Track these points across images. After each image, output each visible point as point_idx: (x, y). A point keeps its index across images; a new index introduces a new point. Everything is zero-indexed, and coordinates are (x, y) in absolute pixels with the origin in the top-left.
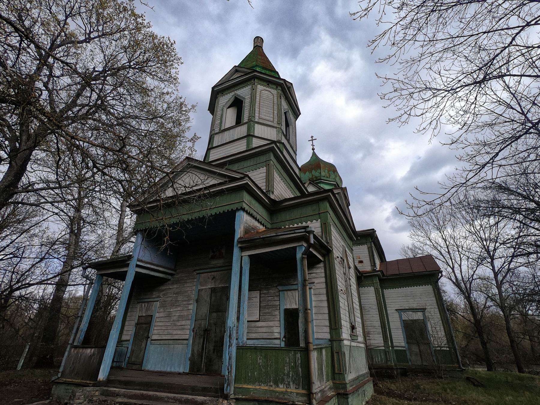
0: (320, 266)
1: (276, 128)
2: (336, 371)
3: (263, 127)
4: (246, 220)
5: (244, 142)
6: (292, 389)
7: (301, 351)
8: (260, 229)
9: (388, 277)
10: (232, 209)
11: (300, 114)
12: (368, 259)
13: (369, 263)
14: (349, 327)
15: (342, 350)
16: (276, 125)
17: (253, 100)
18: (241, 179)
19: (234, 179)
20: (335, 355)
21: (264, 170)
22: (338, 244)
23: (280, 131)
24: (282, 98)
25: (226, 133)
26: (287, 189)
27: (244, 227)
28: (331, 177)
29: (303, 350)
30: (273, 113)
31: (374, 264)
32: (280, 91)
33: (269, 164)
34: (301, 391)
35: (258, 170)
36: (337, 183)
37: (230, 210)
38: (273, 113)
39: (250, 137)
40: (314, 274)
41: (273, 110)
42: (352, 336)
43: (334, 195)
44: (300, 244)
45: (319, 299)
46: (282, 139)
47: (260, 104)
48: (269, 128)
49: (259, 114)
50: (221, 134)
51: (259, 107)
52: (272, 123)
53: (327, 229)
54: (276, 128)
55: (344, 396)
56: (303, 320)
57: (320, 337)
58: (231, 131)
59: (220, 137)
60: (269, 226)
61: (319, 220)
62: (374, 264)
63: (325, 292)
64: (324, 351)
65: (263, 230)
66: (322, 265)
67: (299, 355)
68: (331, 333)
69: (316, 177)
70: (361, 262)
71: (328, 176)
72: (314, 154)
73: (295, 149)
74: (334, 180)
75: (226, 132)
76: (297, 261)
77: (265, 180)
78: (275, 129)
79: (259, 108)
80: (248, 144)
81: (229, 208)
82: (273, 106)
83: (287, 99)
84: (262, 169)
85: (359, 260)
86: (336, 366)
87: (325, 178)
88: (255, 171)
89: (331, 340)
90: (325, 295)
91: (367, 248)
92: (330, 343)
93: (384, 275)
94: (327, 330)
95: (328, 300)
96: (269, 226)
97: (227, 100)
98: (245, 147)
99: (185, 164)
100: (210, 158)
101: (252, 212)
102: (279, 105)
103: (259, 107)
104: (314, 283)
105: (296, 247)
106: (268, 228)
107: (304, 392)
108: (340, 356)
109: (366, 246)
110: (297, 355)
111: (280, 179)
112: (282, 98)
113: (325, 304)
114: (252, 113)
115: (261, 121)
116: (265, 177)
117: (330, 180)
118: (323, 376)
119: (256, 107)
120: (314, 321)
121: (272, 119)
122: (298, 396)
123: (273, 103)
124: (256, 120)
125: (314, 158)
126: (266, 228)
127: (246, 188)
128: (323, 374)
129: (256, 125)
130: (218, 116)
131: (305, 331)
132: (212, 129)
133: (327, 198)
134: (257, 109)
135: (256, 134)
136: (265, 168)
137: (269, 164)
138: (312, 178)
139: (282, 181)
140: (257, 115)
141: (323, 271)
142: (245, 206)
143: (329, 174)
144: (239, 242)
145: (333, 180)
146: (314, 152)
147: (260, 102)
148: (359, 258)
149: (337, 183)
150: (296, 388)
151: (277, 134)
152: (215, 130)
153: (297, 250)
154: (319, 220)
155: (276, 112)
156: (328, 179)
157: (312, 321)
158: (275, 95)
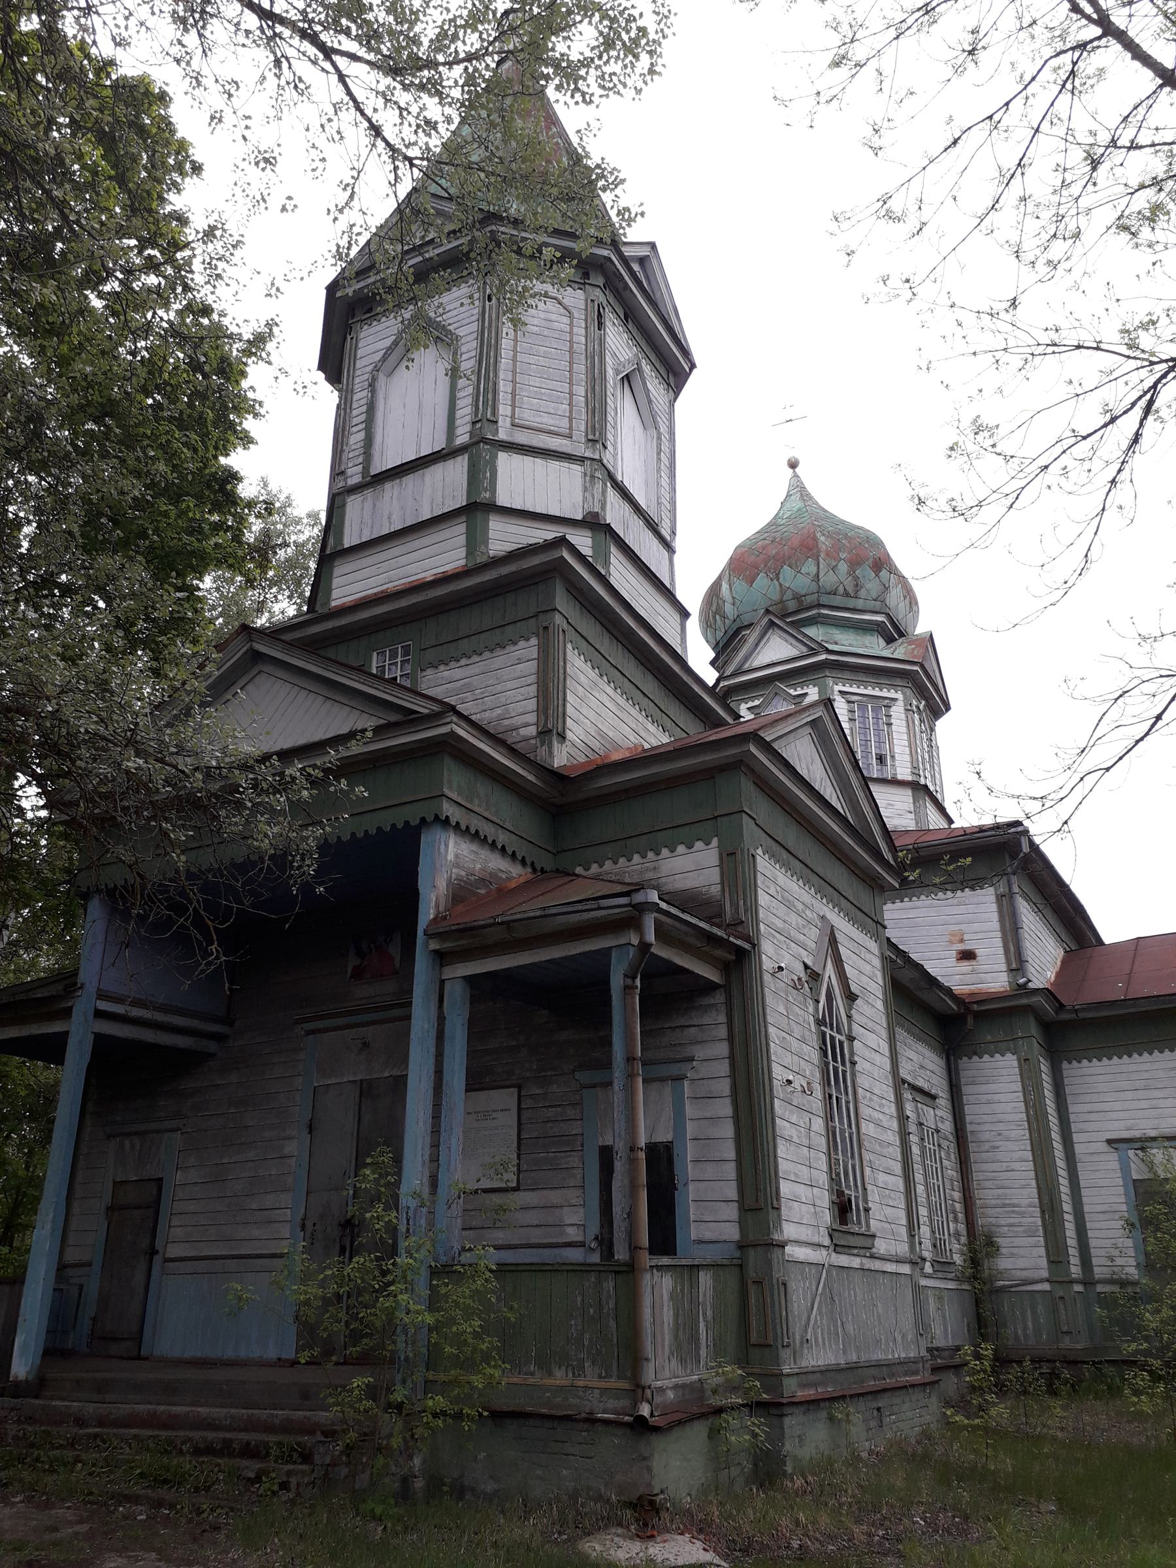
0: (712, 1001)
1: (581, 460)
2: (754, 1338)
3: (528, 460)
4: (457, 856)
5: (456, 535)
6: (591, 1378)
7: (616, 1273)
8: (509, 879)
9: (1081, 1015)
10: (407, 823)
11: (693, 366)
12: (998, 942)
13: (1001, 958)
14: (826, 1203)
15: (776, 1275)
16: (581, 450)
17: (489, 346)
18: (434, 717)
19: (411, 719)
20: (752, 1290)
21: (528, 649)
22: (793, 919)
23: (598, 474)
24: (610, 318)
25: (390, 489)
26: (628, 706)
27: (449, 882)
28: (862, 594)
29: (622, 1269)
30: (571, 394)
31: (1017, 962)
32: (598, 292)
33: (546, 628)
34: (614, 1383)
35: (510, 648)
36: (888, 616)
37: (400, 826)
38: (571, 394)
39: (479, 516)
40: (693, 1030)
41: (571, 384)
42: (836, 1234)
43: (767, 747)
44: (622, 941)
45: (708, 1115)
46: (603, 507)
47: (514, 360)
48: (554, 465)
49: (513, 406)
50: (369, 493)
51: (514, 372)
52: (565, 442)
53: (740, 874)
54: (581, 460)
55: (774, 1411)
56: (626, 1182)
57: (708, 1236)
58: (409, 480)
59: (368, 504)
60: (545, 861)
61: (715, 842)
62: (1017, 962)
63: (727, 1091)
64: (705, 1280)
65: (522, 880)
66: (719, 998)
67: (612, 1284)
68: (742, 1224)
69: (798, 597)
70: (967, 955)
71: (850, 590)
72: (798, 489)
73: (665, 533)
74: (877, 605)
75: (388, 486)
76: (610, 997)
77: (533, 690)
78: (577, 469)
79: (514, 381)
80: (475, 540)
81: (397, 818)
82: (571, 363)
83: (631, 317)
84: (522, 644)
85: (961, 947)
86: (754, 1322)
87: (837, 600)
88: (499, 652)
89: (742, 1246)
90: (728, 1101)
91: (993, 898)
92: (737, 1254)
93: (1062, 1006)
94: (732, 1212)
95: (736, 1118)
96: (545, 861)
97: (388, 342)
98: (462, 552)
99: (239, 650)
100: (335, 594)
101: (476, 824)
102: (596, 355)
103: (514, 372)
104: (692, 1059)
105: (611, 948)
106: (543, 871)
107: (624, 1385)
108: (767, 1294)
109: (991, 890)
110: (605, 1284)
111: (593, 674)
112: (610, 318)
113: (727, 1130)
114: (485, 403)
115: (522, 438)
116: (533, 678)
117: (860, 604)
118: (698, 1348)
119: (501, 375)
120: (691, 1187)
121: (565, 423)
122: (604, 1399)
123: (571, 352)
124: (502, 435)
125: (796, 504)
126: (534, 870)
127: (450, 747)
128: (697, 1341)
129: (502, 457)
130: (360, 396)
131: (629, 1214)
132: (337, 472)
133: (742, 765)
134: (504, 387)
135: (503, 500)
136: (534, 641)
137: (546, 628)
138: (782, 602)
139: (602, 683)
140: (504, 410)
141: (722, 1018)
142: (448, 809)
143: (856, 578)
144: (429, 935)
145: (871, 605)
146: (796, 476)
147: (515, 350)
148: (962, 941)
149: (888, 616)
150: (600, 1376)
151: (585, 489)
152: (349, 472)
153: (613, 960)
154: (715, 842)
155: (580, 390)
156: (851, 603)
157: (686, 1184)
158: (576, 315)
